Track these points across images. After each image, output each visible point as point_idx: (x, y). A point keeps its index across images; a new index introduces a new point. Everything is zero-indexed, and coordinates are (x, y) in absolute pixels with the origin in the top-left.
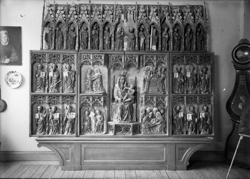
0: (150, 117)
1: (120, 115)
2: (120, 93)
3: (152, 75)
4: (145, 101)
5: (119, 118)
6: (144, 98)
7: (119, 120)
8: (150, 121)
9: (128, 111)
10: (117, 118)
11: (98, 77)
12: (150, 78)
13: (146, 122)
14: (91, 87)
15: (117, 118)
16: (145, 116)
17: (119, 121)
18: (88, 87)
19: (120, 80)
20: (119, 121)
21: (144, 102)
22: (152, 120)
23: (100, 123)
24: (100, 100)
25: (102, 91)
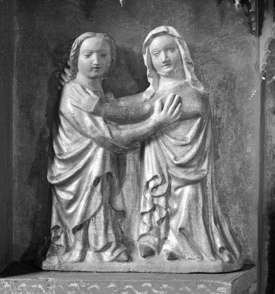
11: (185, 118)
14: (108, 203)
18: (82, 204)
25: (214, 253)
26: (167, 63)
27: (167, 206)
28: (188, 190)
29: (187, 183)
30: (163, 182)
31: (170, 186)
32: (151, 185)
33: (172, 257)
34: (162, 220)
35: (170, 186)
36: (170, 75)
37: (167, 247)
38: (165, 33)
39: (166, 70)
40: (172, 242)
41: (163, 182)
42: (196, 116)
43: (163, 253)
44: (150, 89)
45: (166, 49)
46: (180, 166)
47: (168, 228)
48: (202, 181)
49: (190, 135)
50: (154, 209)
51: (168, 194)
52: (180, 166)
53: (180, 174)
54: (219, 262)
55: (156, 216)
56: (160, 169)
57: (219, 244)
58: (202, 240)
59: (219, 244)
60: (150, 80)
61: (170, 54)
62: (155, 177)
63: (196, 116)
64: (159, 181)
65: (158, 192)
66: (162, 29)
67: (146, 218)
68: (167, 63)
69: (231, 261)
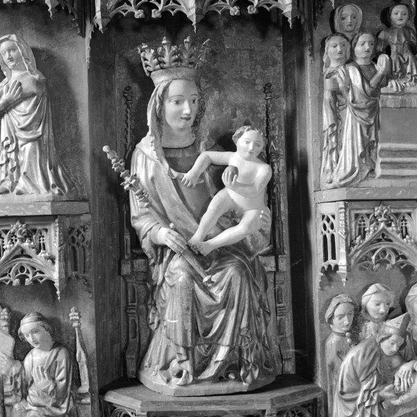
0: (389, 347)
1: (180, 340)
2: (169, 198)
3: (383, 60)
4: (350, 245)
5: (174, 364)
6: (339, 223)
7: (179, 375)
8: (386, 378)
9: (234, 311)
10: (166, 367)
11: (25, 97)
12: (373, 82)
13: (365, 387)
15: (166, 367)
16: (356, 340)
17: (180, 381)
19: (162, 103)
20: (180, 381)
21: (341, 250)
22: (405, 368)
23: (52, 400)
24: (40, 248)
25: (47, 187)
26: (11, 59)
27: (17, 159)
28: (29, 146)
29: (28, 141)
30: (12, 142)
31: (17, 145)
32: (5, 144)
33: (19, 193)
34: (13, 169)
35: (17, 145)
36: (15, 67)
37: (18, 188)
38: (7, 39)
39: (11, 65)
40: (22, 183)
41: (12, 142)
42: (33, 95)
43: (15, 191)
44: (6, 80)
45: (9, 50)
46: (23, 129)
47: (19, 175)
48: (38, 140)
49: (28, 109)
50: (8, 161)
51: (17, 150)
52: (23, 129)
53: (22, 135)
54: (50, 194)
55: (10, 166)
56: (10, 133)
57: (51, 181)
58: (40, 182)
59: (51, 181)
60: (5, 73)
61: (12, 53)
62: (7, 139)
63: (33, 95)
64: (9, 142)
65: (9, 150)
66: (6, 36)
67: (3, 168)
68: (11, 59)
69: (61, 194)
